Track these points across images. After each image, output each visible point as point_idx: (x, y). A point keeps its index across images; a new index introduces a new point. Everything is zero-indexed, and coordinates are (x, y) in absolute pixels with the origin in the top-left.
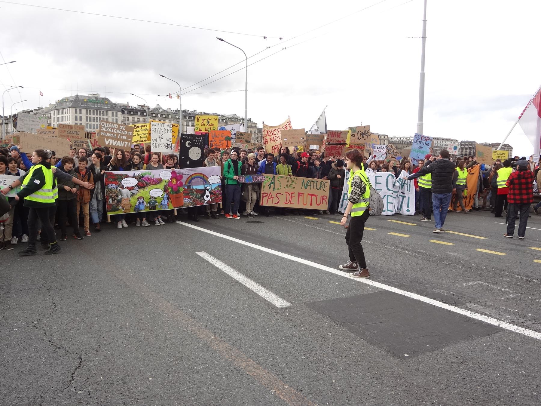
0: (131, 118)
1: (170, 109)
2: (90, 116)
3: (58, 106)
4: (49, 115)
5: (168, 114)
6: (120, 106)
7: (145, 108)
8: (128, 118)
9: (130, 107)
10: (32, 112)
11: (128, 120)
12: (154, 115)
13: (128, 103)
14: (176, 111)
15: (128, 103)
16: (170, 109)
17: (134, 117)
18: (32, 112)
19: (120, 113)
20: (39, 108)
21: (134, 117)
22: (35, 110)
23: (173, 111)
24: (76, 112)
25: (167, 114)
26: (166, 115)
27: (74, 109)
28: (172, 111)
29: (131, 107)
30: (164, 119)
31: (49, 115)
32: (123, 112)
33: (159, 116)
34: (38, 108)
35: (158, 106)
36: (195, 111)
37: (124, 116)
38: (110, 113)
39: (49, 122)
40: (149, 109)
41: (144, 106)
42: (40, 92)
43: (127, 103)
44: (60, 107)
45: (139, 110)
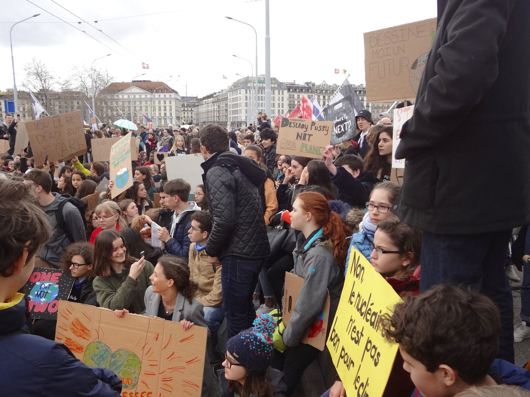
0: (296, 96)
1: (336, 84)
2: (261, 95)
3: (233, 87)
4: (227, 96)
6: (287, 85)
7: (311, 85)
8: (294, 95)
9: (295, 85)
10: (216, 94)
11: (294, 98)
12: (318, 91)
13: (295, 81)
15: (295, 81)
16: (336, 84)
17: (298, 94)
18: (216, 94)
19: (286, 92)
20: (222, 90)
21: (298, 94)
22: (219, 92)
24: (246, 93)
25: (332, 90)
26: (331, 91)
27: (244, 90)
29: (297, 85)
30: (329, 95)
31: (227, 96)
32: (289, 90)
33: (324, 92)
35: (324, 83)
36: (362, 85)
37: (290, 94)
38: (276, 92)
39: (226, 103)
40: (314, 85)
41: (310, 83)
42: (224, 76)
43: (293, 81)
44: (235, 89)
45: (305, 87)
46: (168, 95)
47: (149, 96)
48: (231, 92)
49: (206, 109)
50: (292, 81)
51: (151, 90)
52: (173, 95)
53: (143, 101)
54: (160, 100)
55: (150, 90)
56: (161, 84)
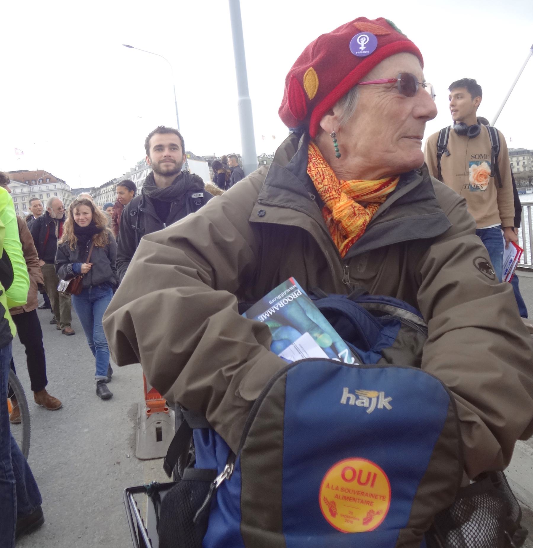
3: (137, 168)
5: (263, 160)
9: (216, 158)
13: (214, 154)
14: (272, 155)
15: (214, 154)
23: (269, 155)
28: (266, 156)
29: (218, 158)
34: (123, 176)
44: (140, 170)
46: (51, 186)
47: (26, 190)
48: (135, 175)
49: (106, 199)
50: (212, 155)
51: (29, 181)
52: (58, 185)
53: (18, 197)
54: (41, 193)
55: (27, 182)
56: (42, 173)
